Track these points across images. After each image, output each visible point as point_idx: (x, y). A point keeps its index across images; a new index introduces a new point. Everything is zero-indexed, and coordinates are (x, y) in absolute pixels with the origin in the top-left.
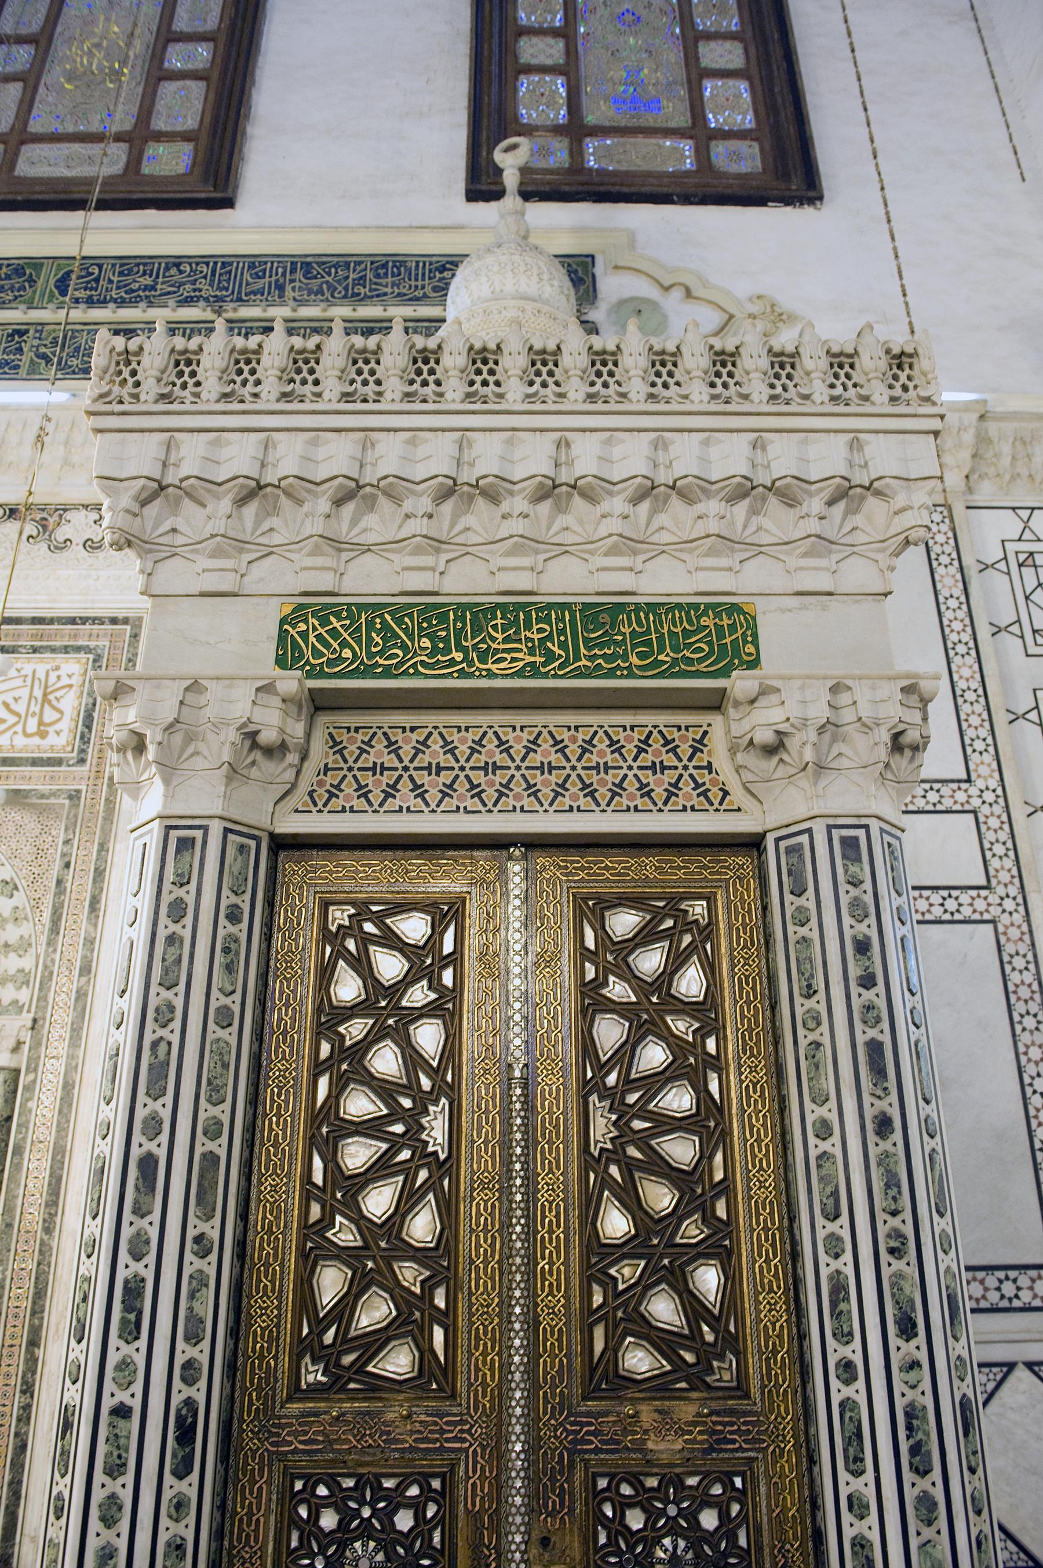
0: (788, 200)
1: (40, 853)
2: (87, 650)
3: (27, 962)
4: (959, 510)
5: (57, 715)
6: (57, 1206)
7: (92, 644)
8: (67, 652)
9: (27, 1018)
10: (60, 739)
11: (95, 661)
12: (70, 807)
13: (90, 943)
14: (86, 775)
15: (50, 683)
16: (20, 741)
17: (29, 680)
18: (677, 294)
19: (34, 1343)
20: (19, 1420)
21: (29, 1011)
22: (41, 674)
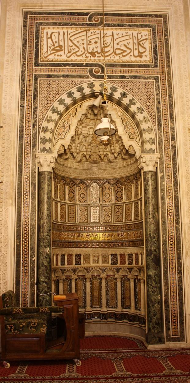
1: (149, 98)
2: (149, 26)
3: (152, 136)
5: (144, 50)
6: (179, 216)
7: (151, 24)
8: (142, 27)
9: (158, 155)
10: (147, 58)
11: (153, 30)
12: (156, 82)
13: (173, 129)
14: (159, 71)
15: (139, 38)
16: (133, 59)
17: (131, 36)
19: (179, 257)
20: (178, 281)
21: (157, 152)
22: (135, 34)
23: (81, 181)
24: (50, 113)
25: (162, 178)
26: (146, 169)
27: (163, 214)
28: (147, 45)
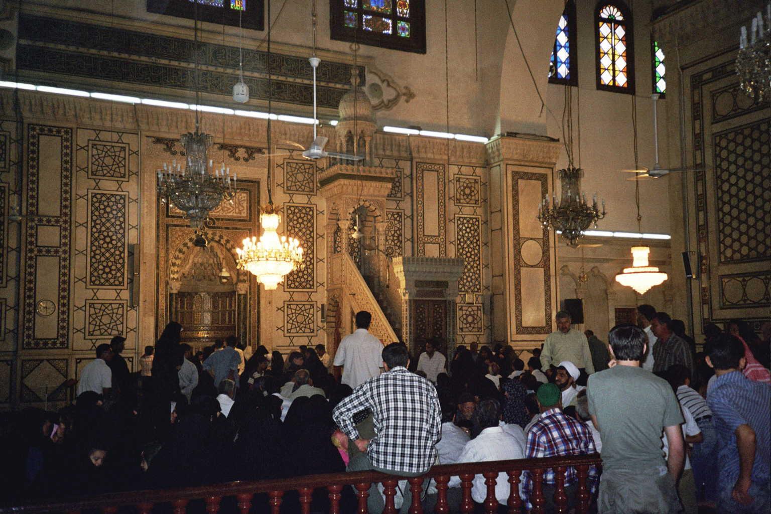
0: (418, 52)
4: (446, 166)
10: (244, 214)
16: (235, 214)
18: (386, 83)
23: (189, 294)
24: (177, 253)
25: (250, 298)
26: (240, 292)
27: (250, 321)
28: (245, 205)
